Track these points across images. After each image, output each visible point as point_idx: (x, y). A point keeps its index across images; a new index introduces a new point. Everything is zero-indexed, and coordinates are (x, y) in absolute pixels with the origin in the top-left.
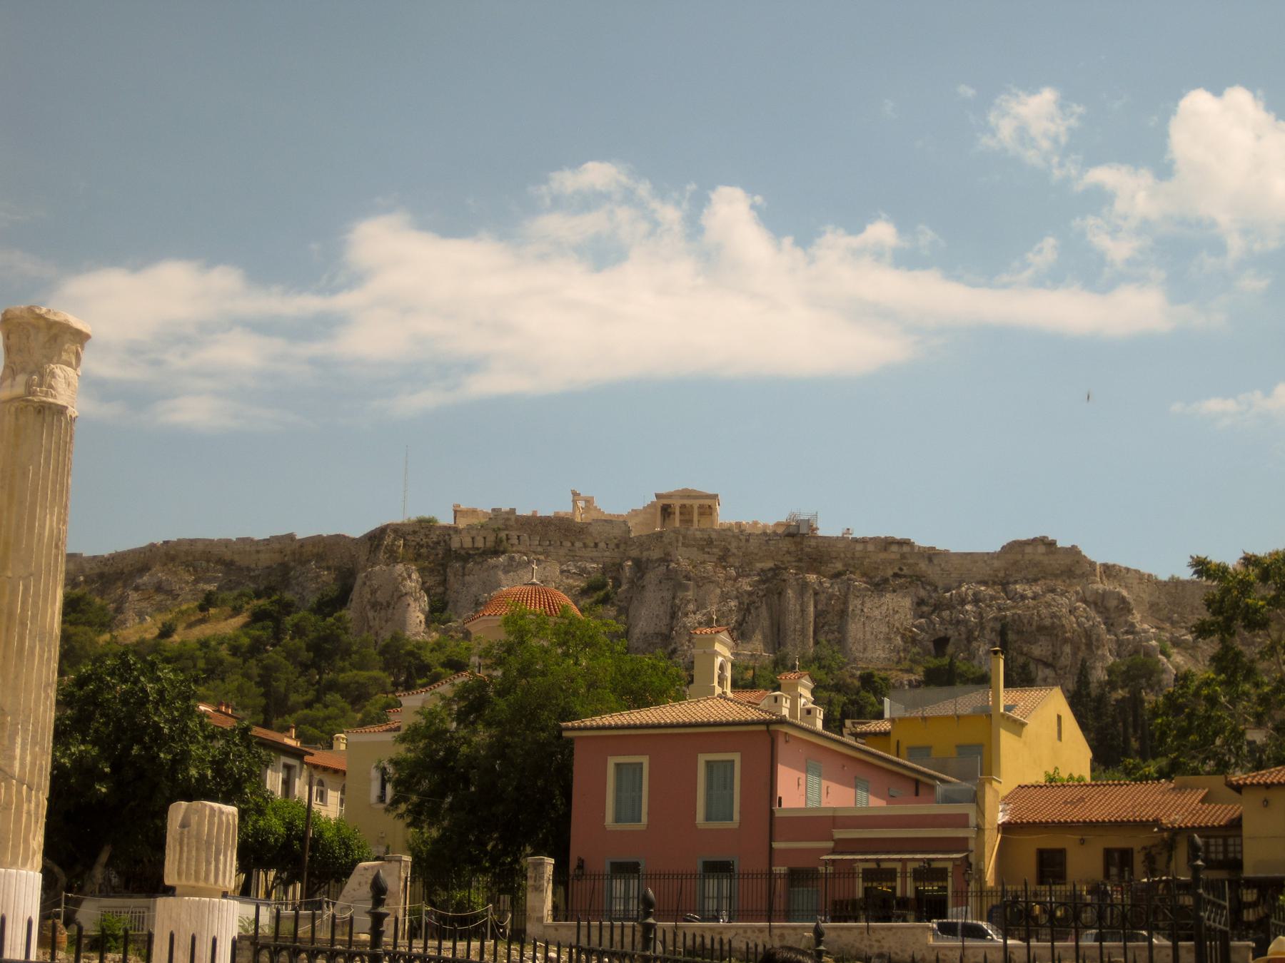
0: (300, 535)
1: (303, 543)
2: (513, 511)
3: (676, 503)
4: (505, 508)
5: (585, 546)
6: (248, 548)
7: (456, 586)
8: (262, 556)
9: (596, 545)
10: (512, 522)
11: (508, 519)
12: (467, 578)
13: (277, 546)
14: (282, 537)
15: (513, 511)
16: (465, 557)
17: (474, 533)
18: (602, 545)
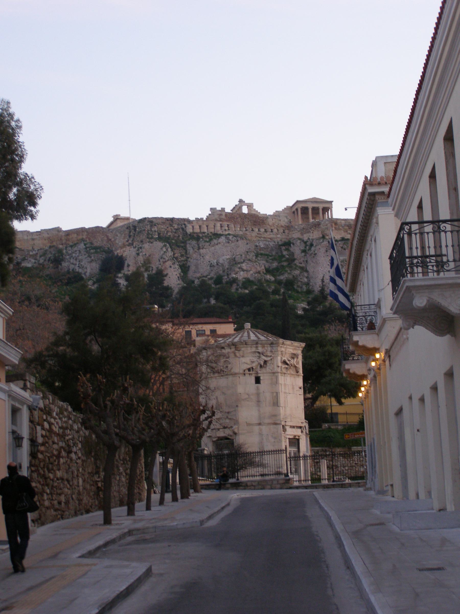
0: (66, 227)
1: (69, 233)
2: (223, 210)
3: (310, 206)
4: (219, 208)
5: (266, 231)
6: (26, 238)
7: (194, 256)
8: (36, 242)
9: (272, 231)
10: (223, 217)
11: (221, 215)
12: (201, 251)
13: (46, 235)
14: (50, 229)
15: (223, 210)
16: (196, 237)
17: (200, 223)
18: (275, 230)
